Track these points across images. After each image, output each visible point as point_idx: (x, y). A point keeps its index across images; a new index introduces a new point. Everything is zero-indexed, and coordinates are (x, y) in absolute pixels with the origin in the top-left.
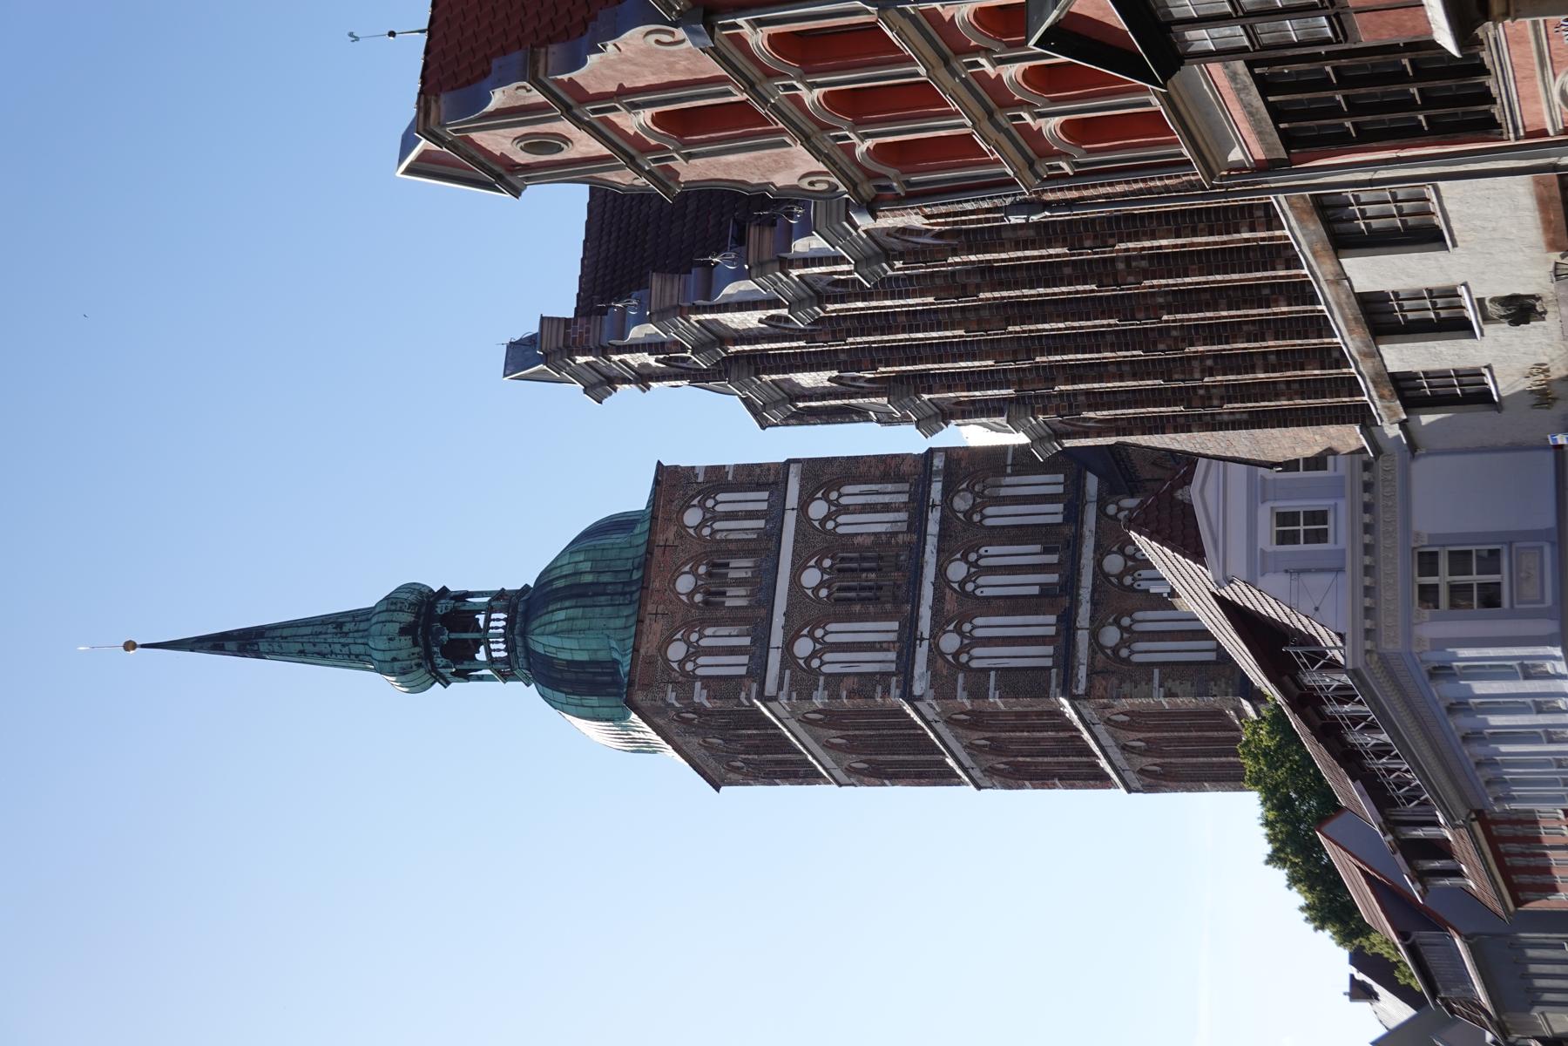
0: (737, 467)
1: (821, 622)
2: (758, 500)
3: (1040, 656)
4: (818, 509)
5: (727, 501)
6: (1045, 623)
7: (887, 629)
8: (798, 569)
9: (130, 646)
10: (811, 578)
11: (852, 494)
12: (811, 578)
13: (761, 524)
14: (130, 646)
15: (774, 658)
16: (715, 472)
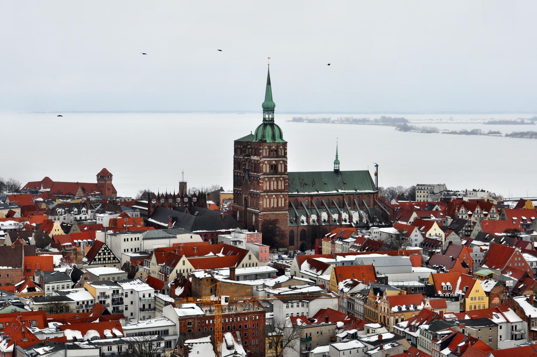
0: (287, 152)
1: (269, 164)
2: (283, 154)
3: (265, 189)
4: (281, 162)
5: (283, 151)
6: (268, 188)
7: (268, 171)
8: (275, 161)
9: (269, 65)
10: (274, 162)
11: (283, 166)
12: (274, 162)
13: (280, 155)
14: (269, 65)
15: (265, 159)
16: (286, 149)
